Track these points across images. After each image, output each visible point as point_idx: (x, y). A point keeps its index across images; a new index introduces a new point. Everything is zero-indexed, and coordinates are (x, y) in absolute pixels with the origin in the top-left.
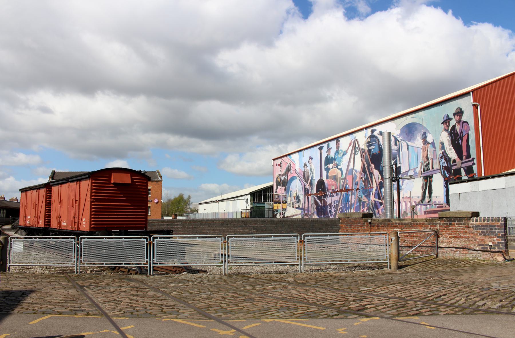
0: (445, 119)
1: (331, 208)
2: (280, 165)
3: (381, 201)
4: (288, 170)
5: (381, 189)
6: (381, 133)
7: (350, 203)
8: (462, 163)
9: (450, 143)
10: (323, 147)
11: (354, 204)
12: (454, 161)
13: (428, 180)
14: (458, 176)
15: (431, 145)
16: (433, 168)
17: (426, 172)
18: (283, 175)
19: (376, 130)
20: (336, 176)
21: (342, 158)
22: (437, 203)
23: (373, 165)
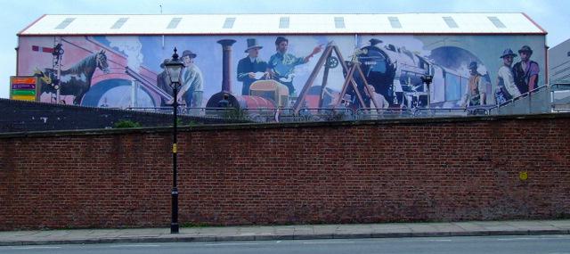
2: (56, 52)
4: (90, 67)
6: (392, 48)
9: (513, 80)
10: (233, 42)
18: (63, 73)
19: (381, 42)
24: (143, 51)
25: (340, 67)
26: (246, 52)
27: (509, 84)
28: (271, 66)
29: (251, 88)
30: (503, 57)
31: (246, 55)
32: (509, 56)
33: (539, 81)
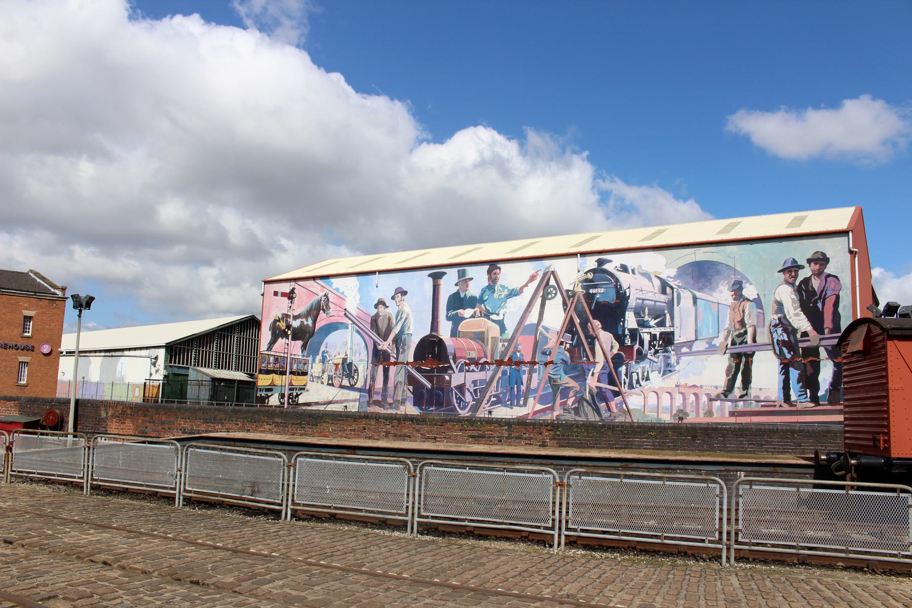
1: (463, 394)
2: (290, 296)
3: (616, 389)
5: (617, 367)
6: (624, 269)
7: (523, 388)
8: (821, 339)
9: (798, 304)
11: (535, 391)
12: (805, 334)
14: (811, 358)
15: (753, 304)
16: (754, 341)
17: (738, 346)
18: (295, 318)
19: (610, 261)
20: (483, 333)
21: (505, 301)
22: (762, 398)
23: (597, 323)
24: (360, 290)
25: (559, 299)
26: (456, 285)
28: (481, 300)
29: (459, 329)
30: (780, 272)
31: (455, 289)
32: (792, 269)
33: (841, 305)
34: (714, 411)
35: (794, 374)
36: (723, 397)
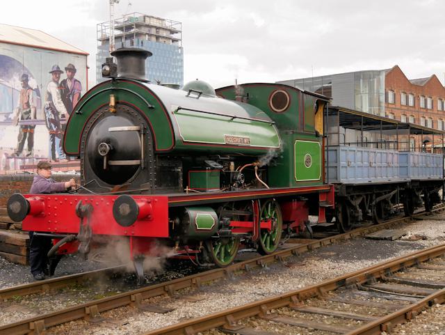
0: (55, 69)
9: (60, 96)
12: (63, 116)
13: (27, 133)
16: (35, 118)
22: (40, 157)
27: (57, 100)
30: (50, 73)
32: (56, 72)
34: (10, 165)
35: (58, 141)
36: (16, 156)
